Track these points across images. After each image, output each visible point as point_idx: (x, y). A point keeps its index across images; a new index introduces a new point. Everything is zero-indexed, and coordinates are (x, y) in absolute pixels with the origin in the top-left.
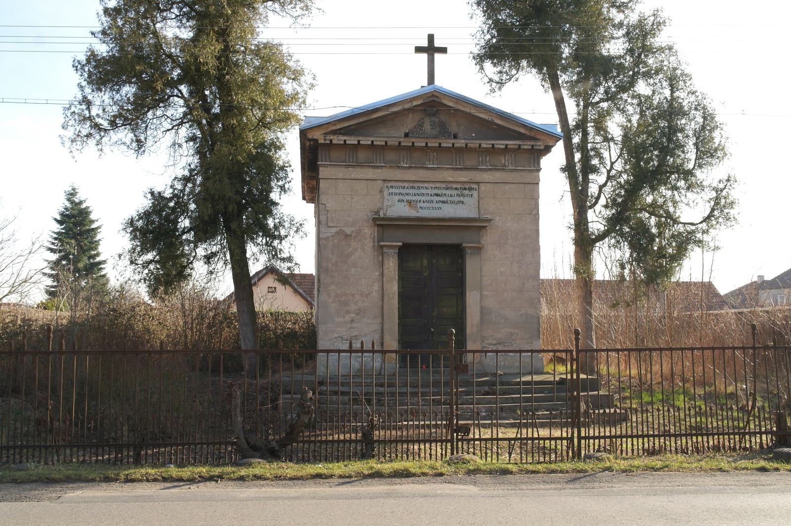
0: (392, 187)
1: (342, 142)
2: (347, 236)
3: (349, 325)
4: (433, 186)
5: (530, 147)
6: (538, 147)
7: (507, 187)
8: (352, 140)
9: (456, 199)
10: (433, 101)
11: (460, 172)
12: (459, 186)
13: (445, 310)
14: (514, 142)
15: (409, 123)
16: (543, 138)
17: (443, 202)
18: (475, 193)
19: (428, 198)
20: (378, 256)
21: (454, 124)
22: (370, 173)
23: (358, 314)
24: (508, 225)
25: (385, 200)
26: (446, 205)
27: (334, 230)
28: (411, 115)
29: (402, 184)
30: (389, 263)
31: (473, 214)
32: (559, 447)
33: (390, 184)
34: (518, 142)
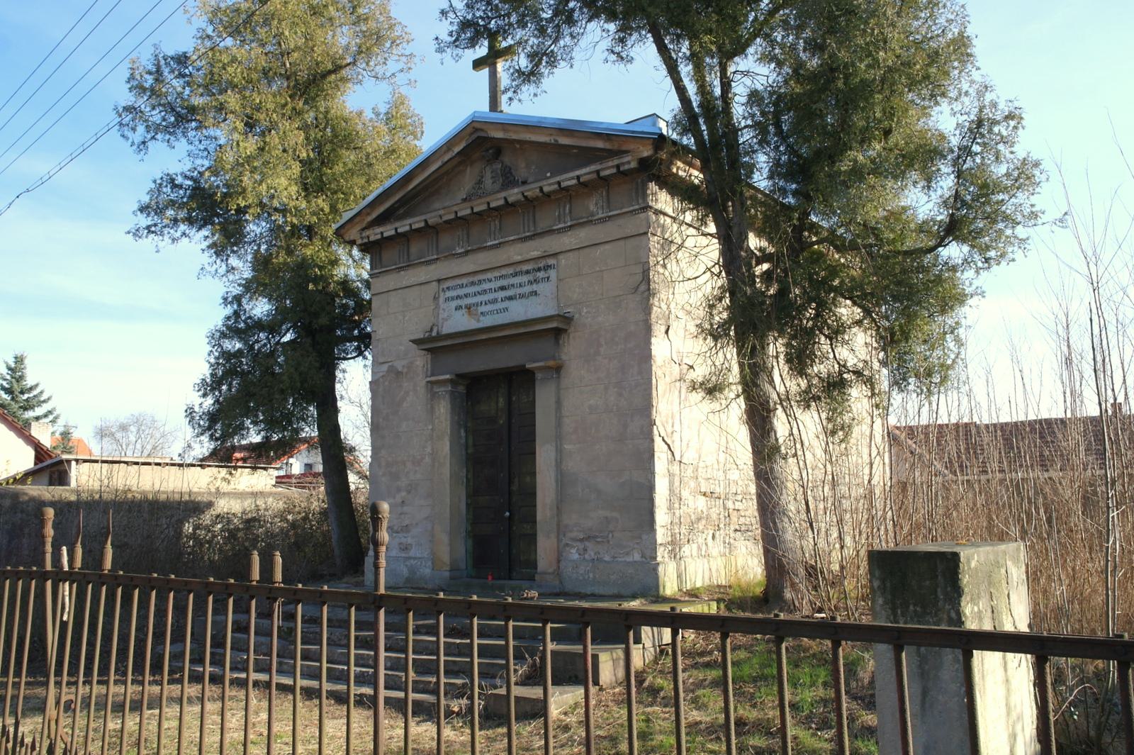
2: (398, 373)
4: (497, 274)
6: (626, 167)
7: (598, 251)
8: (388, 230)
9: (527, 289)
10: (478, 137)
17: (510, 298)
21: (523, 165)
22: (421, 274)
23: (409, 492)
24: (600, 319)
25: (441, 311)
29: (459, 282)
34: (593, 168)
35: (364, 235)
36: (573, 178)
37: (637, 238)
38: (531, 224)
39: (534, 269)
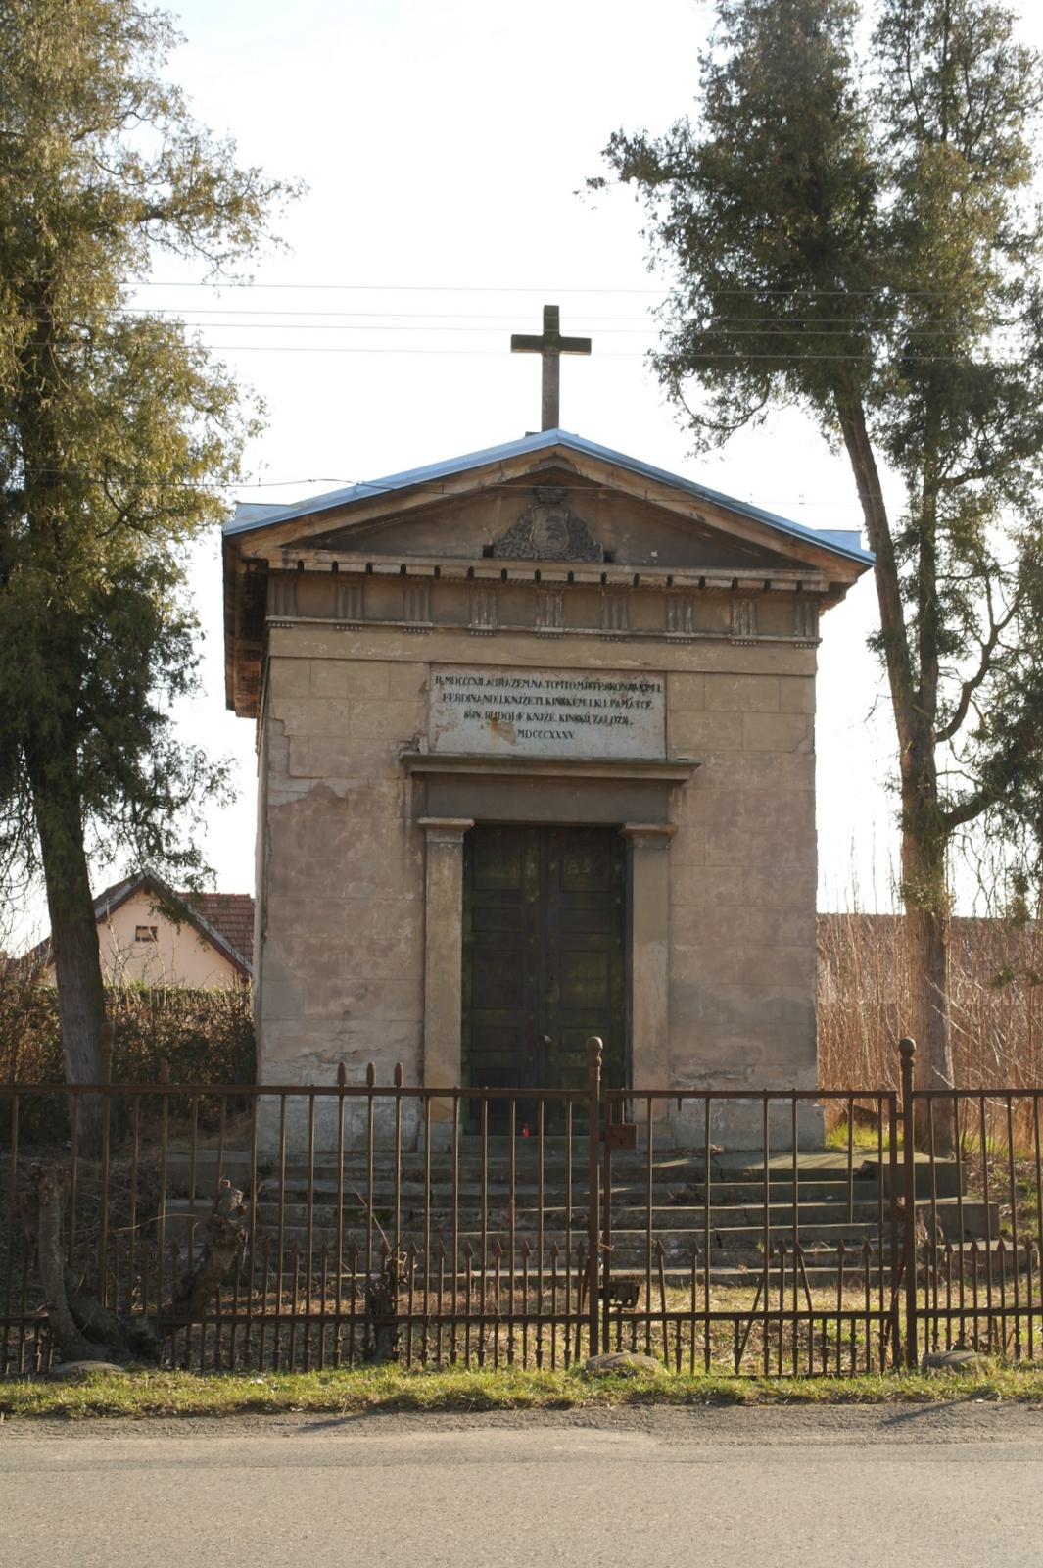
0: (450, 680)
1: (328, 568)
2: (337, 802)
3: (339, 1025)
4: (553, 678)
5: (794, 587)
6: (812, 587)
7: (737, 684)
9: (610, 712)
10: (556, 469)
11: (620, 646)
12: (616, 680)
13: (580, 988)
14: (754, 574)
15: (496, 523)
16: (825, 564)
17: (578, 719)
18: (657, 699)
19: (541, 709)
20: (414, 853)
21: (607, 526)
22: (395, 645)
24: (738, 777)
25: (433, 713)
26: (584, 727)
27: (303, 786)
28: (499, 502)
29: (476, 675)
30: (439, 871)
31: (652, 750)
32: (861, 1336)
33: (444, 674)
34: (763, 574)
35: (293, 556)
36: (727, 579)
37: (799, 680)
38: (624, 618)
39: (622, 685)
